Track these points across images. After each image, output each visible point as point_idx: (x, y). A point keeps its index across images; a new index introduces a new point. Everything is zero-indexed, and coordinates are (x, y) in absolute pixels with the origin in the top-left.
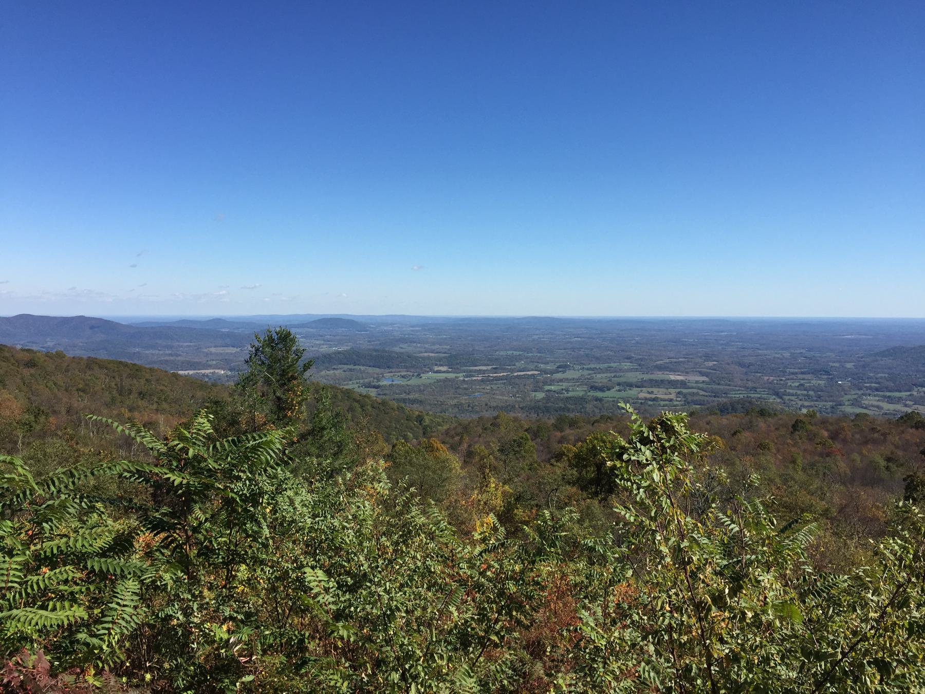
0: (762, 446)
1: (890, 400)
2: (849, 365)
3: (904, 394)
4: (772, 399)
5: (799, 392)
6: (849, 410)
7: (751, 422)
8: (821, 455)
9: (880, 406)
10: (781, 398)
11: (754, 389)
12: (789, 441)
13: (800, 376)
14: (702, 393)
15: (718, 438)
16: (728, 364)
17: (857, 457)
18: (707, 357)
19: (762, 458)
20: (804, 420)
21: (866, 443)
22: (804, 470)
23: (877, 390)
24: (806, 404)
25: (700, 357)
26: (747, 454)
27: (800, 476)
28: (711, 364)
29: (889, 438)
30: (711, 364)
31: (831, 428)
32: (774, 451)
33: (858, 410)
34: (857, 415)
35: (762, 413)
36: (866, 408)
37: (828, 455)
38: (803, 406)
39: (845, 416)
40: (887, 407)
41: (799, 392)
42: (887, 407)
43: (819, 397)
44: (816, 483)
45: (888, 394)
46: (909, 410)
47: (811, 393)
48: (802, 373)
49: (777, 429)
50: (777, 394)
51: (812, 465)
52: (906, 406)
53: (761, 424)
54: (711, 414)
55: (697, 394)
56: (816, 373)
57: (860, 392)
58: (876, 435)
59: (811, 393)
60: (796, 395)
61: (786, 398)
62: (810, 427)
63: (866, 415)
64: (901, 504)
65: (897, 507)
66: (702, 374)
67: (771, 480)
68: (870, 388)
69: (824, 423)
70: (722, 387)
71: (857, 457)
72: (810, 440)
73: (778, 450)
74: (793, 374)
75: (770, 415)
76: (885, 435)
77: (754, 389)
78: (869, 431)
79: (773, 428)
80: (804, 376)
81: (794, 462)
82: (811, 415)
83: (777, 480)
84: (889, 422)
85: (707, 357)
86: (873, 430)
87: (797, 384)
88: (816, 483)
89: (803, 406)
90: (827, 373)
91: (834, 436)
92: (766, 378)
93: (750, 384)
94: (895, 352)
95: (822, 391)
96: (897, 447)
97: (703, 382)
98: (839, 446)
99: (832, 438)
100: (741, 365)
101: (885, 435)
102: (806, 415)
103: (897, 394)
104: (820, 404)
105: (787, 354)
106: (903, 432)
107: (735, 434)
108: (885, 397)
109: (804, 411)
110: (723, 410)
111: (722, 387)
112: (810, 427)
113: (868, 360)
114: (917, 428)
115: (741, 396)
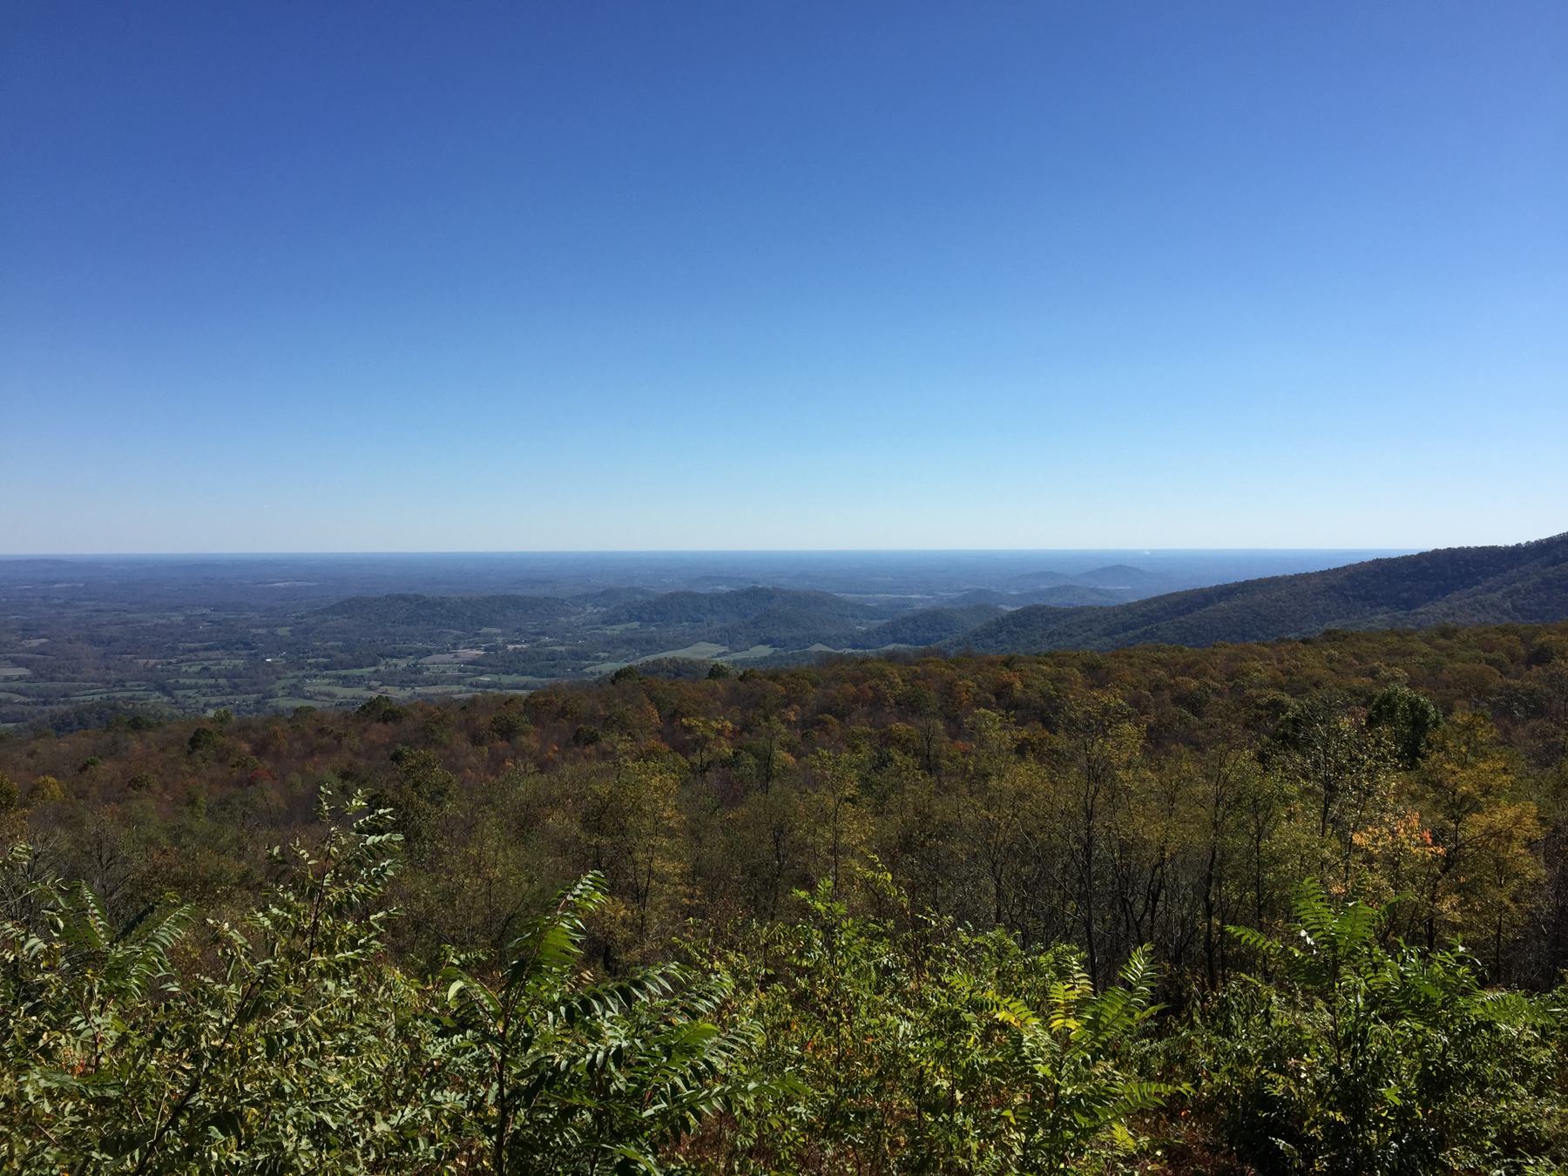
0: (136, 784)
1: (347, 682)
2: (283, 631)
3: (366, 671)
4: (156, 699)
5: (201, 682)
6: (285, 703)
7: (115, 743)
8: (239, 784)
9: (330, 693)
10: (170, 694)
11: (121, 683)
12: (185, 767)
13: (201, 654)
14: (17, 698)
15: (51, 780)
16: (70, 641)
17: (295, 778)
18: (28, 631)
19: (135, 805)
20: (210, 727)
21: (311, 754)
22: (210, 812)
23: (327, 667)
24: (214, 700)
25: (13, 632)
26: (108, 801)
27: (203, 824)
28: (35, 643)
29: (345, 741)
30: (35, 643)
31: (254, 736)
32: (158, 788)
33: (299, 703)
34: (297, 710)
35: (136, 724)
36: (310, 698)
37: (251, 782)
38: (208, 705)
39: (278, 713)
40: (343, 692)
41: (201, 682)
42: (343, 692)
43: (236, 686)
44: (230, 833)
45: (343, 673)
46: (374, 695)
47: (222, 681)
48: (207, 649)
49: (163, 750)
50: (163, 689)
51: (224, 804)
52: (370, 688)
53: (135, 744)
54: (37, 738)
55: (9, 702)
56: (228, 646)
57: (301, 674)
58: (326, 740)
59: (222, 681)
60: (196, 686)
61: (179, 693)
62: (220, 740)
63: (310, 709)
64: (276, 850)
65: (271, 855)
66: (17, 663)
67: (150, 841)
68: (317, 666)
69: (244, 729)
70: (57, 685)
71: (295, 778)
72: (221, 761)
73: (165, 786)
74: (190, 651)
75: (149, 727)
76: (338, 738)
77: (121, 683)
78: (315, 735)
79: (155, 749)
80: (209, 654)
81: (192, 802)
82: (222, 719)
83: (163, 839)
84: (346, 715)
85: (28, 631)
86: (321, 731)
87: (197, 668)
88: (230, 833)
89: (208, 705)
90: (247, 645)
91: (260, 750)
92: (142, 662)
93: (113, 675)
94: (352, 606)
95: (239, 676)
96: (357, 754)
97: (20, 678)
98: (268, 764)
99: (256, 753)
100: (94, 641)
101: (338, 738)
102: (213, 721)
103: (357, 672)
104: (238, 699)
105: (178, 618)
106: (365, 730)
107: (85, 767)
108: (339, 677)
109: (211, 713)
110: (62, 726)
111: (57, 685)
112: (220, 740)
113: (313, 620)
114: (385, 722)
115: (97, 698)
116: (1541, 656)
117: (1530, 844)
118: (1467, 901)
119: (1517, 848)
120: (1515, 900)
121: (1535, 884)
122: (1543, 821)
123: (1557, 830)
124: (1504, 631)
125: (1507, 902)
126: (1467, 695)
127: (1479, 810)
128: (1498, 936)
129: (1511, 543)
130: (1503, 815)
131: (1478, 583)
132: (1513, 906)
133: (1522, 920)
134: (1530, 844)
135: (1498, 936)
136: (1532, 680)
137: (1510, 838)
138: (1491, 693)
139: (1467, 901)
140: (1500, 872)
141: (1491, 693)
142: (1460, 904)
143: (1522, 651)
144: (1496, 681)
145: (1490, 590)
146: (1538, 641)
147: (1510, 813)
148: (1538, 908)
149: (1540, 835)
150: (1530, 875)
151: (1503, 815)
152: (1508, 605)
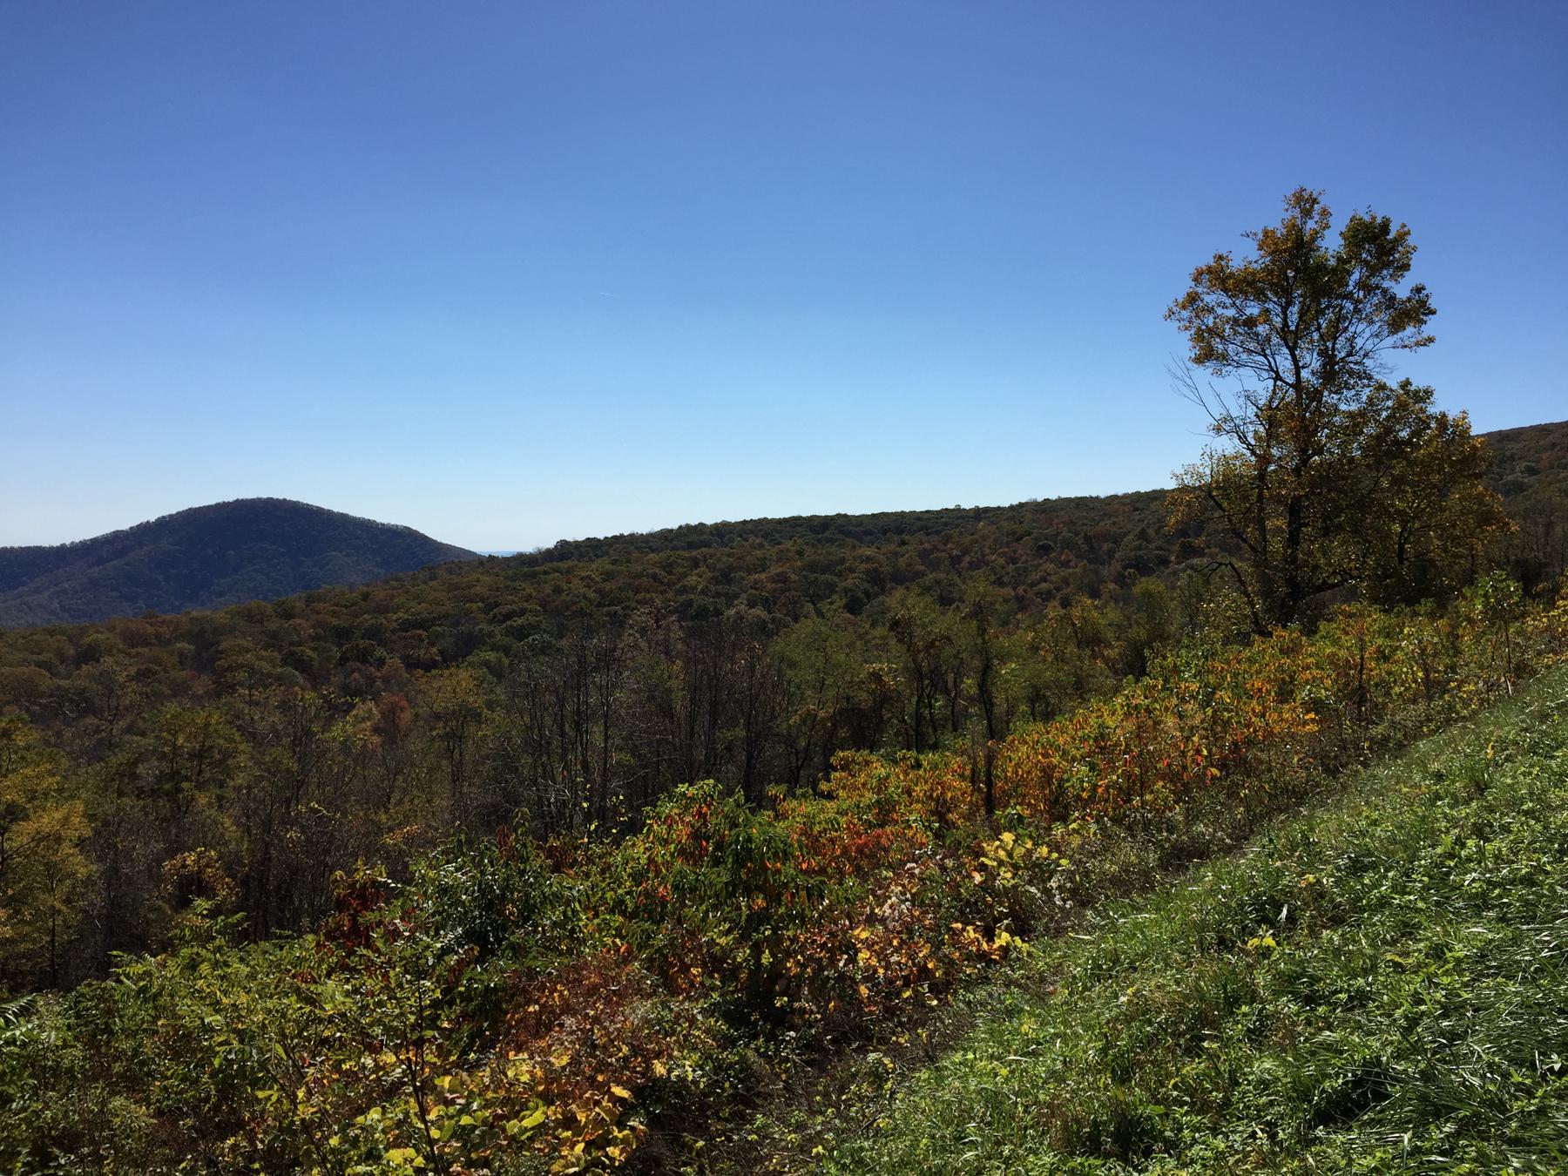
116: (90, 655)
117: (81, 843)
118: (17, 912)
119: (66, 848)
120: (68, 901)
121: (88, 882)
122: (92, 818)
123: (106, 824)
124: (52, 633)
125: (57, 905)
126: (17, 701)
127: (26, 818)
128: (53, 941)
129: (56, 543)
130: (48, 820)
131: (24, 584)
132: (64, 908)
133: (75, 919)
134: (81, 843)
135: (53, 941)
136: (83, 678)
137: (59, 840)
138: (42, 695)
139: (17, 912)
140: (51, 877)
141: (42, 695)
142: (10, 917)
143: (71, 651)
144: (46, 682)
145: (36, 591)
146: (87, 640)
147: (57, 815)
148: (92, 904)
149: (88, 833)
150: (82, 872)
151: (48, 820)
152: (55, 605)
